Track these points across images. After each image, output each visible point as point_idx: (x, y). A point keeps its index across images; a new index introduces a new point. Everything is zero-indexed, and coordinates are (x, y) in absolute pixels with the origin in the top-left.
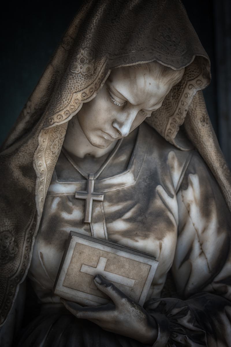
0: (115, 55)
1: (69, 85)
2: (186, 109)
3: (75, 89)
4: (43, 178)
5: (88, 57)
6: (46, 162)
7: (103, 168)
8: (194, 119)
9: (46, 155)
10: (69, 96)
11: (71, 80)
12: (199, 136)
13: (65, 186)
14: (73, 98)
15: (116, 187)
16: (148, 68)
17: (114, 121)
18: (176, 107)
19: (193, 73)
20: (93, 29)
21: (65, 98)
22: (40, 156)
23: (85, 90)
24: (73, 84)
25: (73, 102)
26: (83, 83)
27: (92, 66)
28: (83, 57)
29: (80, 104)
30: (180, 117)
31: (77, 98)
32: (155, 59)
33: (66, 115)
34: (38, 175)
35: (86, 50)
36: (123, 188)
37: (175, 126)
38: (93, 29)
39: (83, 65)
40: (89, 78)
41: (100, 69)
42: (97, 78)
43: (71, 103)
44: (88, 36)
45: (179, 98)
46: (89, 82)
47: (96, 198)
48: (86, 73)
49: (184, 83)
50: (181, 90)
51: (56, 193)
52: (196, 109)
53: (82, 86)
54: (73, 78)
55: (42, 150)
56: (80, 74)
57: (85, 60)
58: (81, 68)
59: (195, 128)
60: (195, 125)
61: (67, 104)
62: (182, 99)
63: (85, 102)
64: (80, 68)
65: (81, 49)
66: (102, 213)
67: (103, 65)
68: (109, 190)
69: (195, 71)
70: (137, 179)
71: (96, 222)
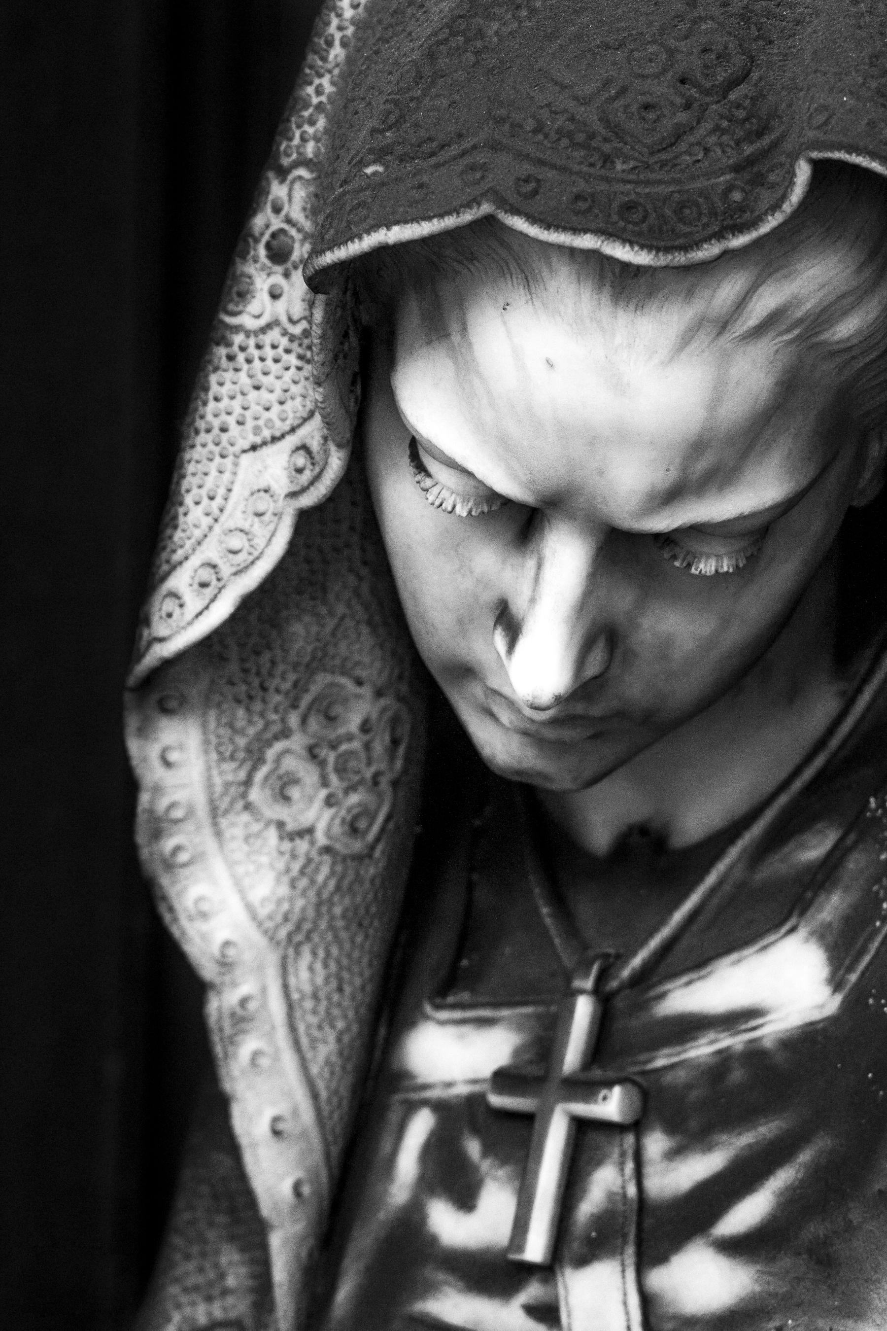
1: (212, 405)
3: (250, 423)
4: (246, 988)
5: (307, 225)
6: (242, 893)
7: (678, 916)
9: (233, 845)
10: (214, 473)
11: (220, 373)
13: (461, 1037)
14: (236, 488)
15: (712, 1035)
16: (513, 266)
20: (337, 43)
22: (183, 857)
23: (302, 432)
24: (232, 398)
25: (241, 507)
26: (294, 389)
29: (278, 515)
31: (263, 485)
32: (486, 208)
34: (208, 971)
35: (300, 178)
36: (752, 1041)
38: (337, 43)
39: (287, 275)
43: (227, 512)
44: (310, 90)
47: (582, 1109)
51: (420, 1080)
53: (289, 406)
54: (231, 358)
55: (178, 814)
57: (297, 246)
58: (275, 295)
63: (307, 500)
64: (266, 297)
65: (271, 175)
66: (625, 1204)
68: (679, 1053)
70: (853, 978)
71: (582, 1262)
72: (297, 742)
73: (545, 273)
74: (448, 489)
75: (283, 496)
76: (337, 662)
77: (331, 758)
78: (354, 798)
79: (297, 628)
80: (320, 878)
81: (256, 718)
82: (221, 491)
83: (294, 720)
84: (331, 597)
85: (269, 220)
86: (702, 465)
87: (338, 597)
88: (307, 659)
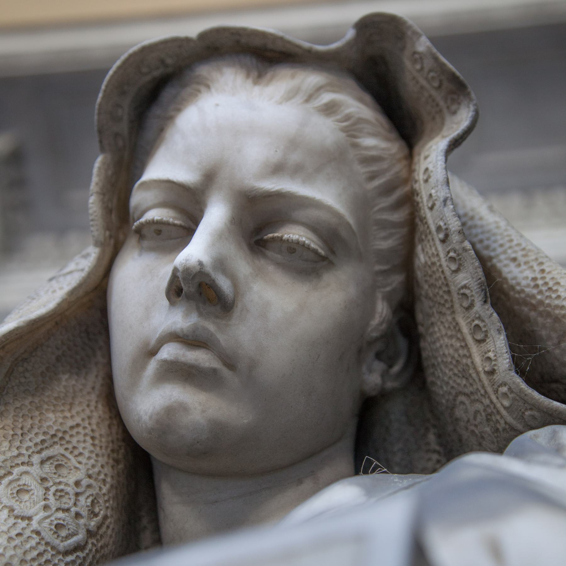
8: (554, 296)
52: (543, 271)
72: (35, 470)
76: (70, 446)
77: (53, 489)
78: (60, 515)
79: (51, 415)
80: (28, 546)
81: (14, 449)
83: (36, 459)
84: (74, 412)
86: (295, 157)
87: (78, 413)
88: (52, 432)
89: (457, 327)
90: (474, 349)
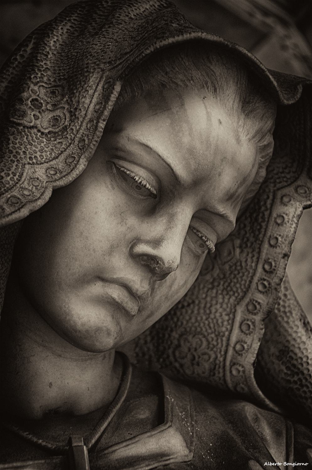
0: (126, 54)
2: (284, 252)
8: (285, 319)
10: (14, 167)
12: (304, 360)
15: (147, 463)
17: (137, 241)
18: (253, 265)
19: (283, 175)
20: (51, 53)
21: (6, 171)
23: (54, 162)
27: (65, 111)
28: (37, 97)
30: (269, 284)
33: (11, 205)
35: (43, 86)
37: (253, 323)
38: (51, 53)
40: (60, 137)
41: (87, 101)
42: (84, 124)
45: (261, 236)
46: (61, 146)
48: (50, 129)
49: (268, 198)
50: (264, 215)
53: (44, 154)
56: (35, 130)
57: (44, 105)
58: (36, 117)
59: (292, 342)
60: (291, 335)
61: (11, 184)
62: (269, 234)
63: (61, 183)
64: (32, 116)
67: (100, 81)
69: (287, 171)
73: (225, 88)
74: (143, 178)
75: (45, 182)
82: (18, 174)
85: (31, 95)
89: (234, 313)
90: (236, 331)
